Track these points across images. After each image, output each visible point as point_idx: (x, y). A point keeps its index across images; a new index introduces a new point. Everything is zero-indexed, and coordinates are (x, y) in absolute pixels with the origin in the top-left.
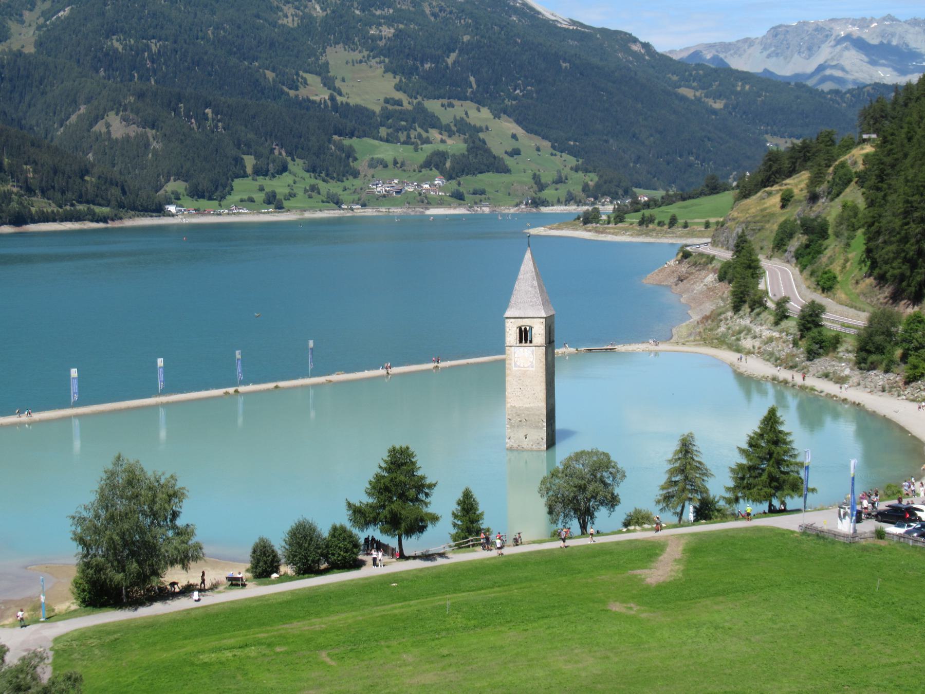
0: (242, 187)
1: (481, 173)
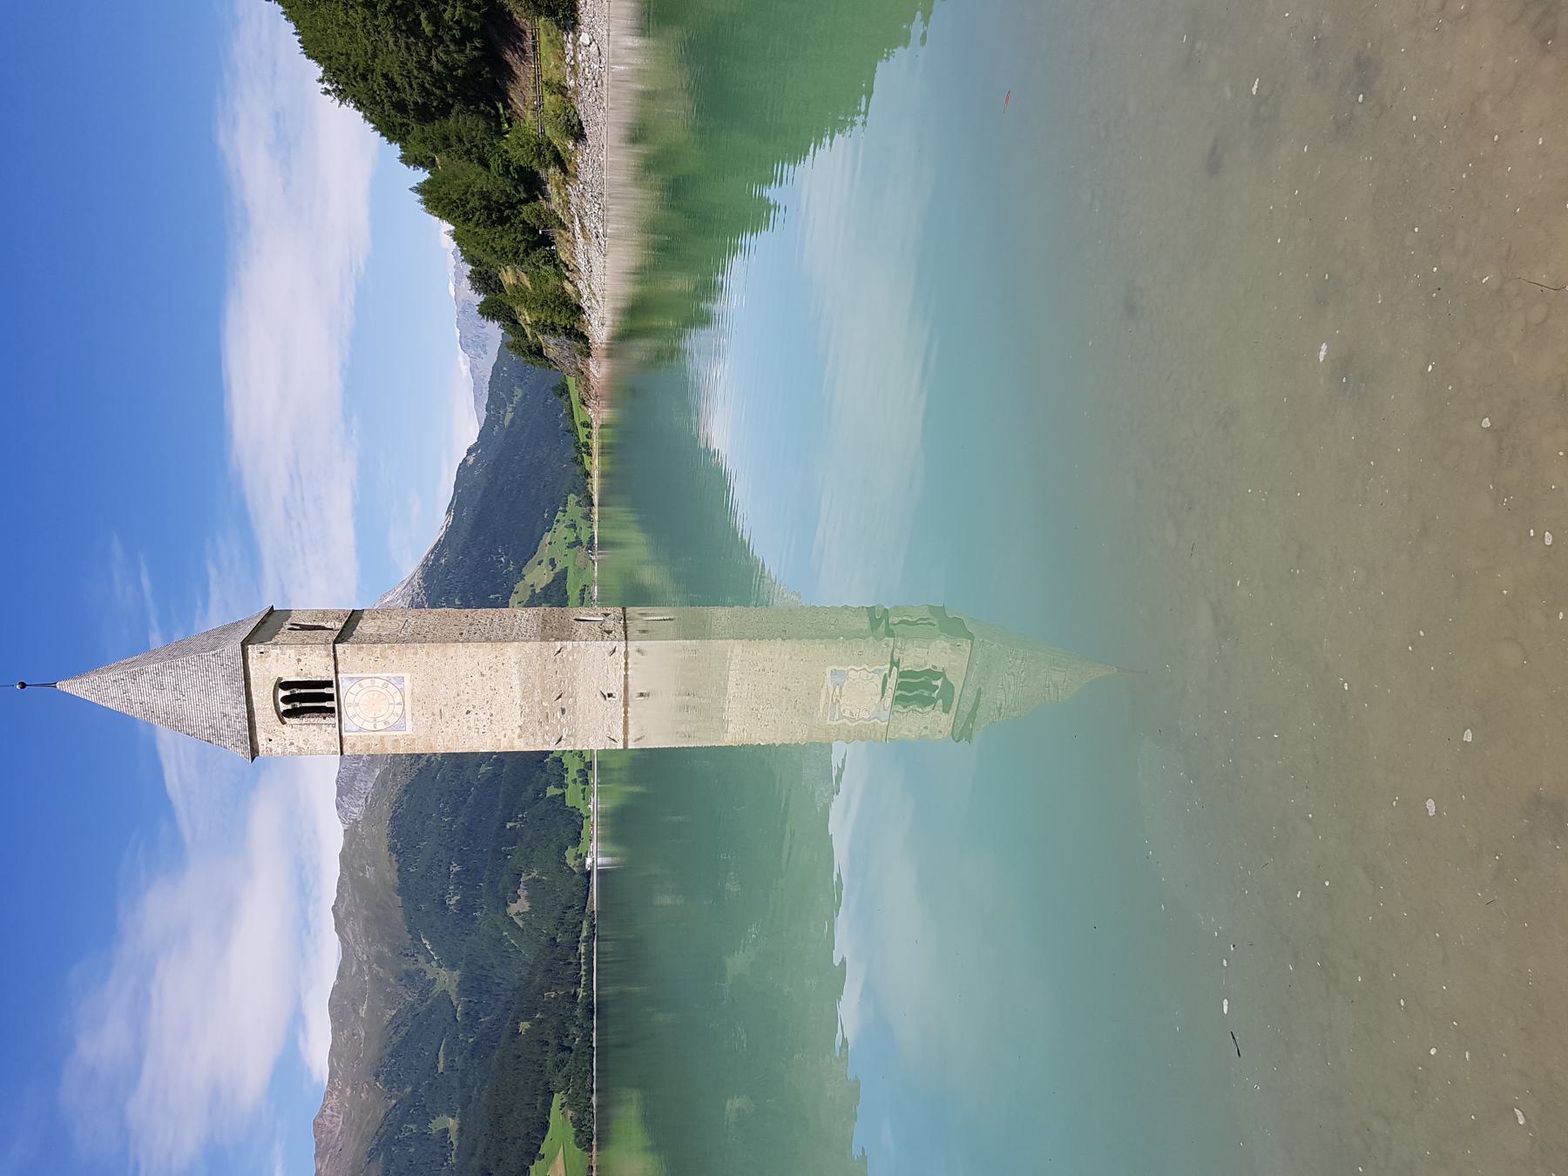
0: (572, 798)
1: (566, 593)
